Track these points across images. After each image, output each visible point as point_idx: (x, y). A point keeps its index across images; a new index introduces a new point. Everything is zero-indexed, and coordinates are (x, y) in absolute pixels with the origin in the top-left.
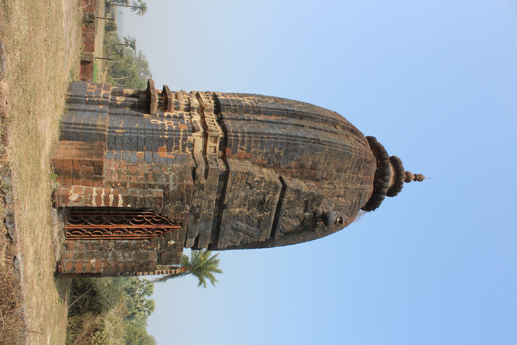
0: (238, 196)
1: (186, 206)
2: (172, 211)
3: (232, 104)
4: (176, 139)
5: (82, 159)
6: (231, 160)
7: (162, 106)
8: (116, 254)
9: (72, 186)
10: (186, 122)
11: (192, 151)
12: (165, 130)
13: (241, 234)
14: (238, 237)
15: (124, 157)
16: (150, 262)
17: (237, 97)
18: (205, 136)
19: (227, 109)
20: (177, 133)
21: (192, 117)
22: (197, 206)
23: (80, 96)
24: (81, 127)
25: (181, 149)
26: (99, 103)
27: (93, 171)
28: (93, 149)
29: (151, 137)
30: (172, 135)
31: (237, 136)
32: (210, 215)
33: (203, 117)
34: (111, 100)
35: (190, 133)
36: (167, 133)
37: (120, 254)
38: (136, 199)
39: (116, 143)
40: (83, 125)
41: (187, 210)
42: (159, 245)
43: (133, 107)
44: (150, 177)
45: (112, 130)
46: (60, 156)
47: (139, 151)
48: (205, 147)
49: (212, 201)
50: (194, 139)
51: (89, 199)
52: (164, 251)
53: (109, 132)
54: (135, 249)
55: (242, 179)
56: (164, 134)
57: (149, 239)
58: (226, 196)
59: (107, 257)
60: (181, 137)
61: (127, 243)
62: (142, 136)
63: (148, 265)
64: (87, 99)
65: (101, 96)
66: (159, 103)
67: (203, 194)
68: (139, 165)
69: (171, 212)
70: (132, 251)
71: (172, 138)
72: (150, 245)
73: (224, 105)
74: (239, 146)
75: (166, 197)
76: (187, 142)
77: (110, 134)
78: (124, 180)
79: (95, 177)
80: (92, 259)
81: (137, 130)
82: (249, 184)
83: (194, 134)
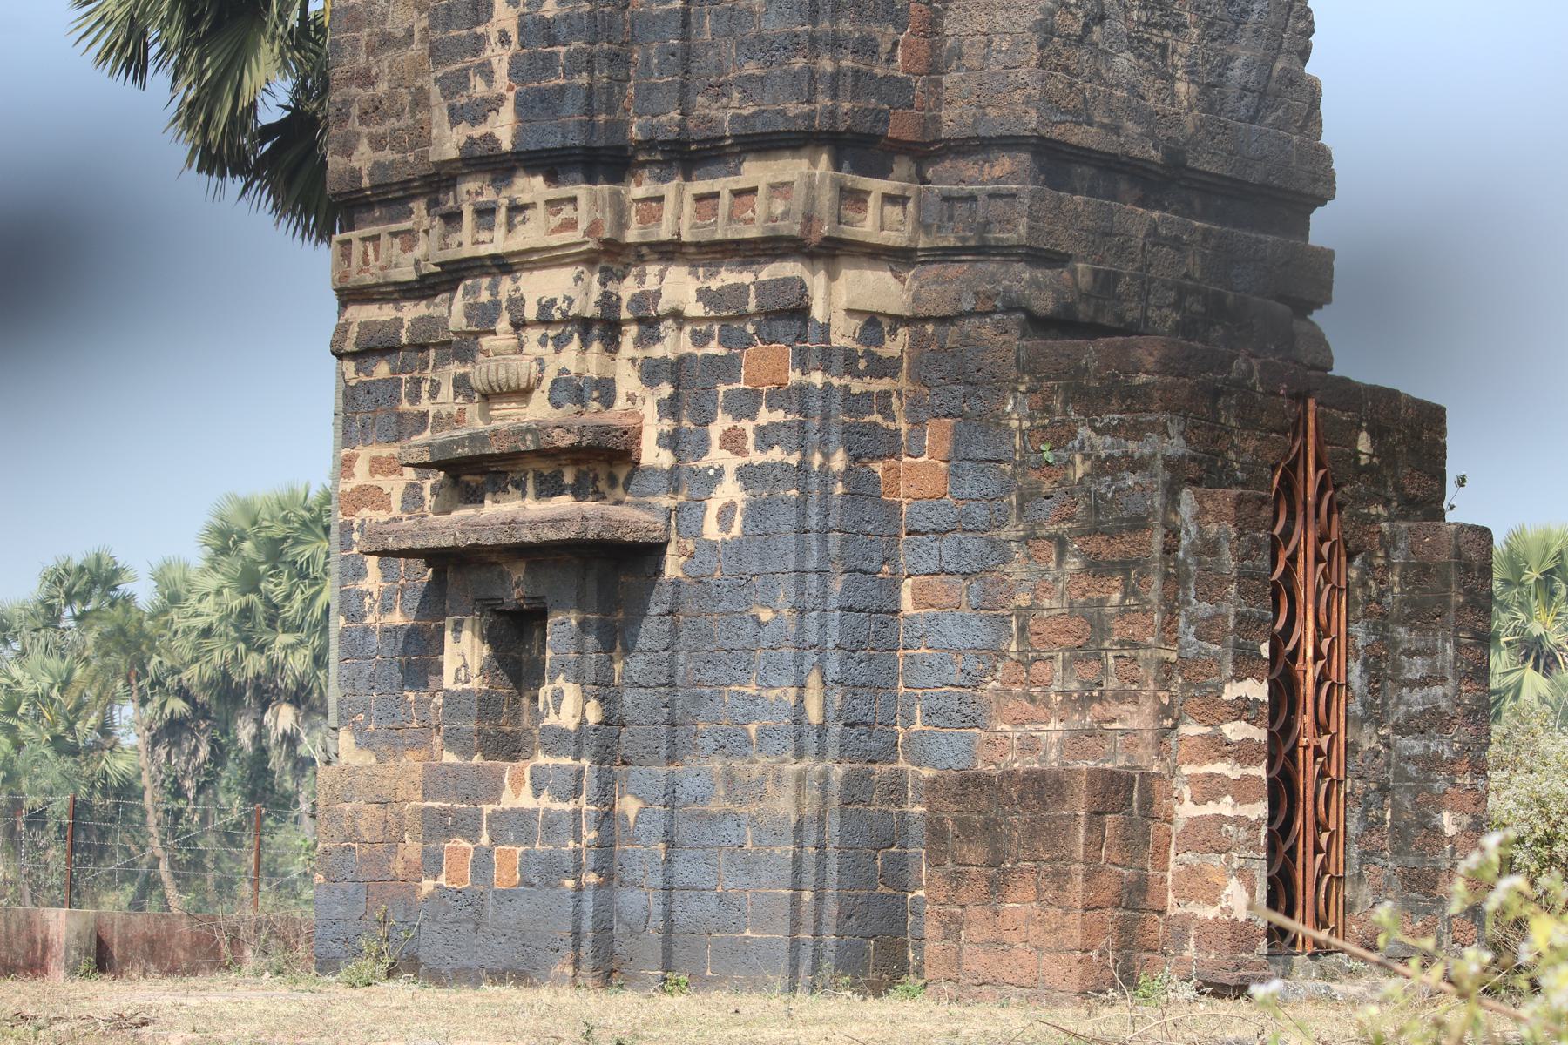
0: (1133, 89)
1: (1234, 375)
2: (1251, 444)
3: (583, 79)
4: (848, 411)
5: (1078, 868)
6: (946, 114)
7: (596, 478)
8: (1409, 717)
9: (1170, 912)
10: (714, 348)
11: (898, 320)
12: (803, 468)
13: (1279, 65)
14: (1292, 82)
15: (958, 678)
16: (1458, 554)
17: (491, 30)
18: (832, 252)
19: (610, 109)
20: (815, 404)
21: (677, 316)
22: (1176, 306)
23: (577, 915)
24: (808, 896)
25: (885, 384)
26: (607, 818)
27: (1120, 816)
28: (990, 825)
29: (844, 542)
30: (824, 429)
31: (835, 77)
32: (1206, 234)
33: (670, 252)
34: (577, 758)
35: (812, 333)
36: (817, 459)
37: (1416, 699)
38: (1244, 615)
39: (869, 719)
40: (797, 887)
41: (1250, 372)
42: (1373, 511)
43: (614, 634)
44: (1113, 549)
45: (811, 743)
46: (1059, 969)
47: (897, 602)
48: (876, 254)
49: (1153, 231)
50: (850, 312)
51: (1243, 834)
52: (1396, 488)
53: (821, 754)
54: (1385, 628)
55: (1065, 68)
56: (825, 472)
57: (1350, 557)
58: (1136, 152)
59: (1430, 762)
60: (836, 382)
61: (1365, 664)
62: (837, 585)
63: (1466, 567)
64: (592, 878)
65: (569, 806)
66: (579, 493)
67: (1133, 277)
68: (1023, 600)
69: (1255, 451)
70: (1395, 644)
71: (847, 429)
72: (1372, 554)
73: (590, 127)
74: (879, 71)
75: (1208, 471)
76: (860, 349)
77: (834, 751)
78: (1149, 674)
79: (1140, 808)
80: (1437, 831)
81: (802, 612)
82: (1086, 25)
83: (818, 313)
